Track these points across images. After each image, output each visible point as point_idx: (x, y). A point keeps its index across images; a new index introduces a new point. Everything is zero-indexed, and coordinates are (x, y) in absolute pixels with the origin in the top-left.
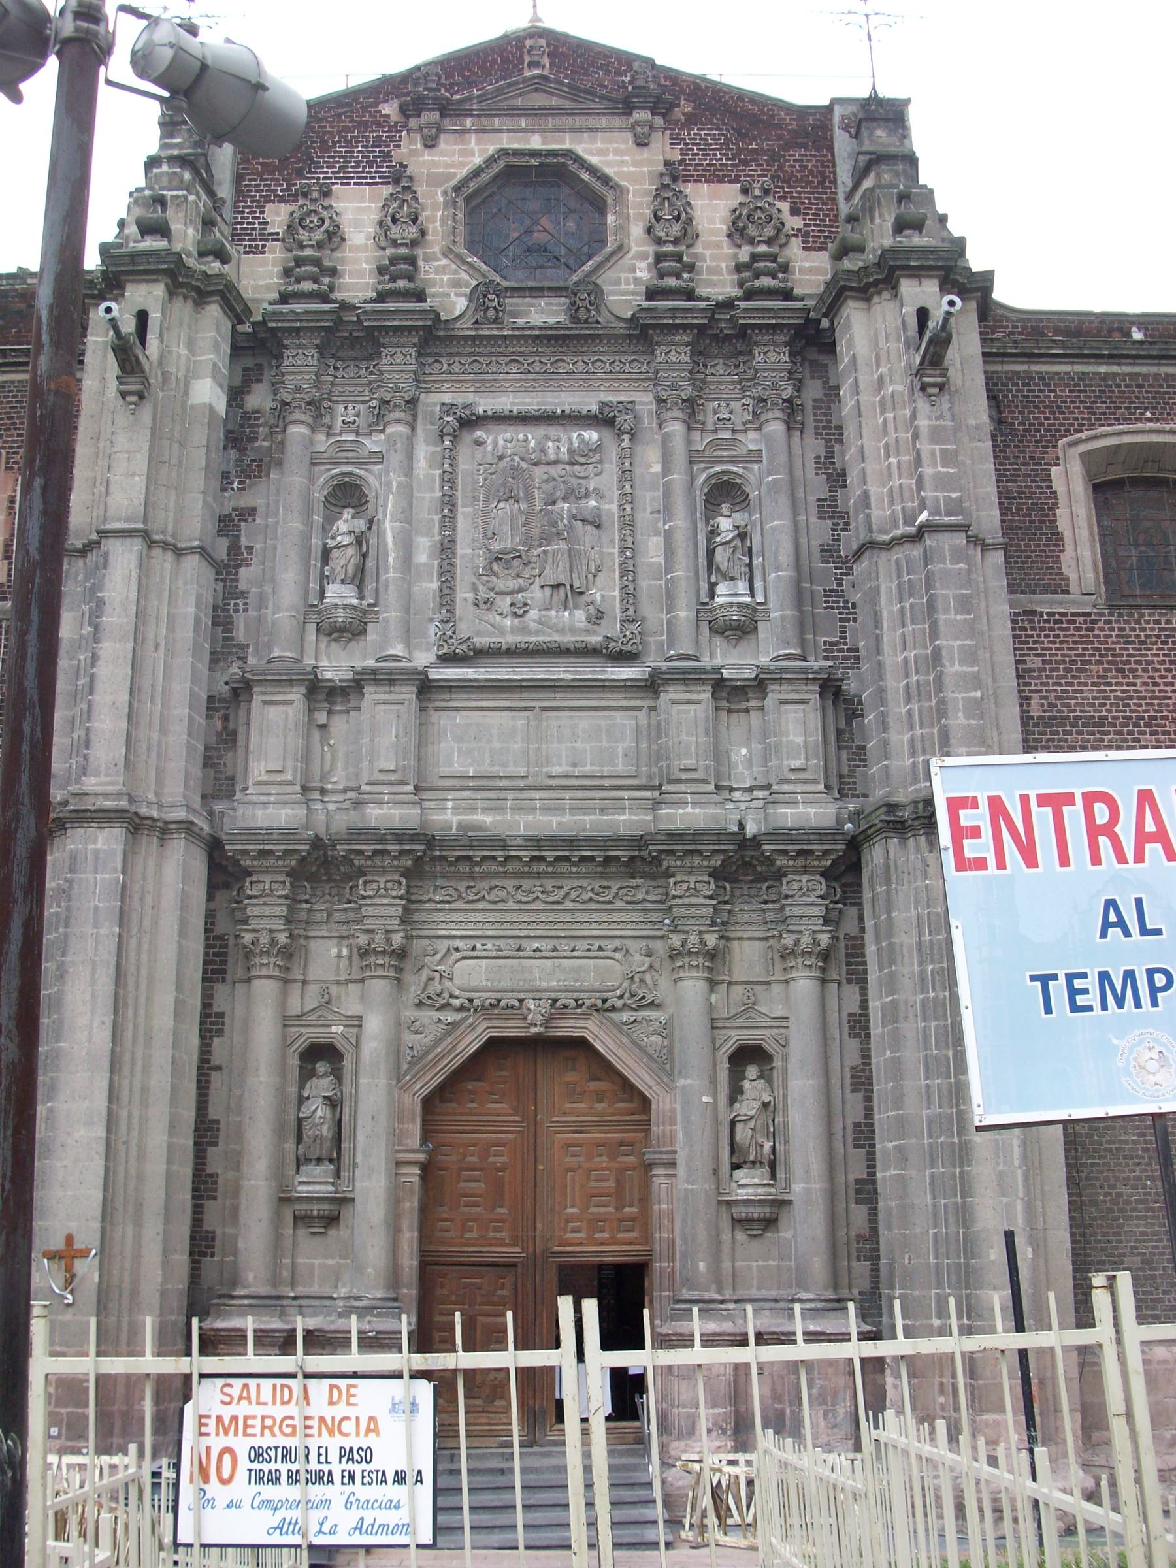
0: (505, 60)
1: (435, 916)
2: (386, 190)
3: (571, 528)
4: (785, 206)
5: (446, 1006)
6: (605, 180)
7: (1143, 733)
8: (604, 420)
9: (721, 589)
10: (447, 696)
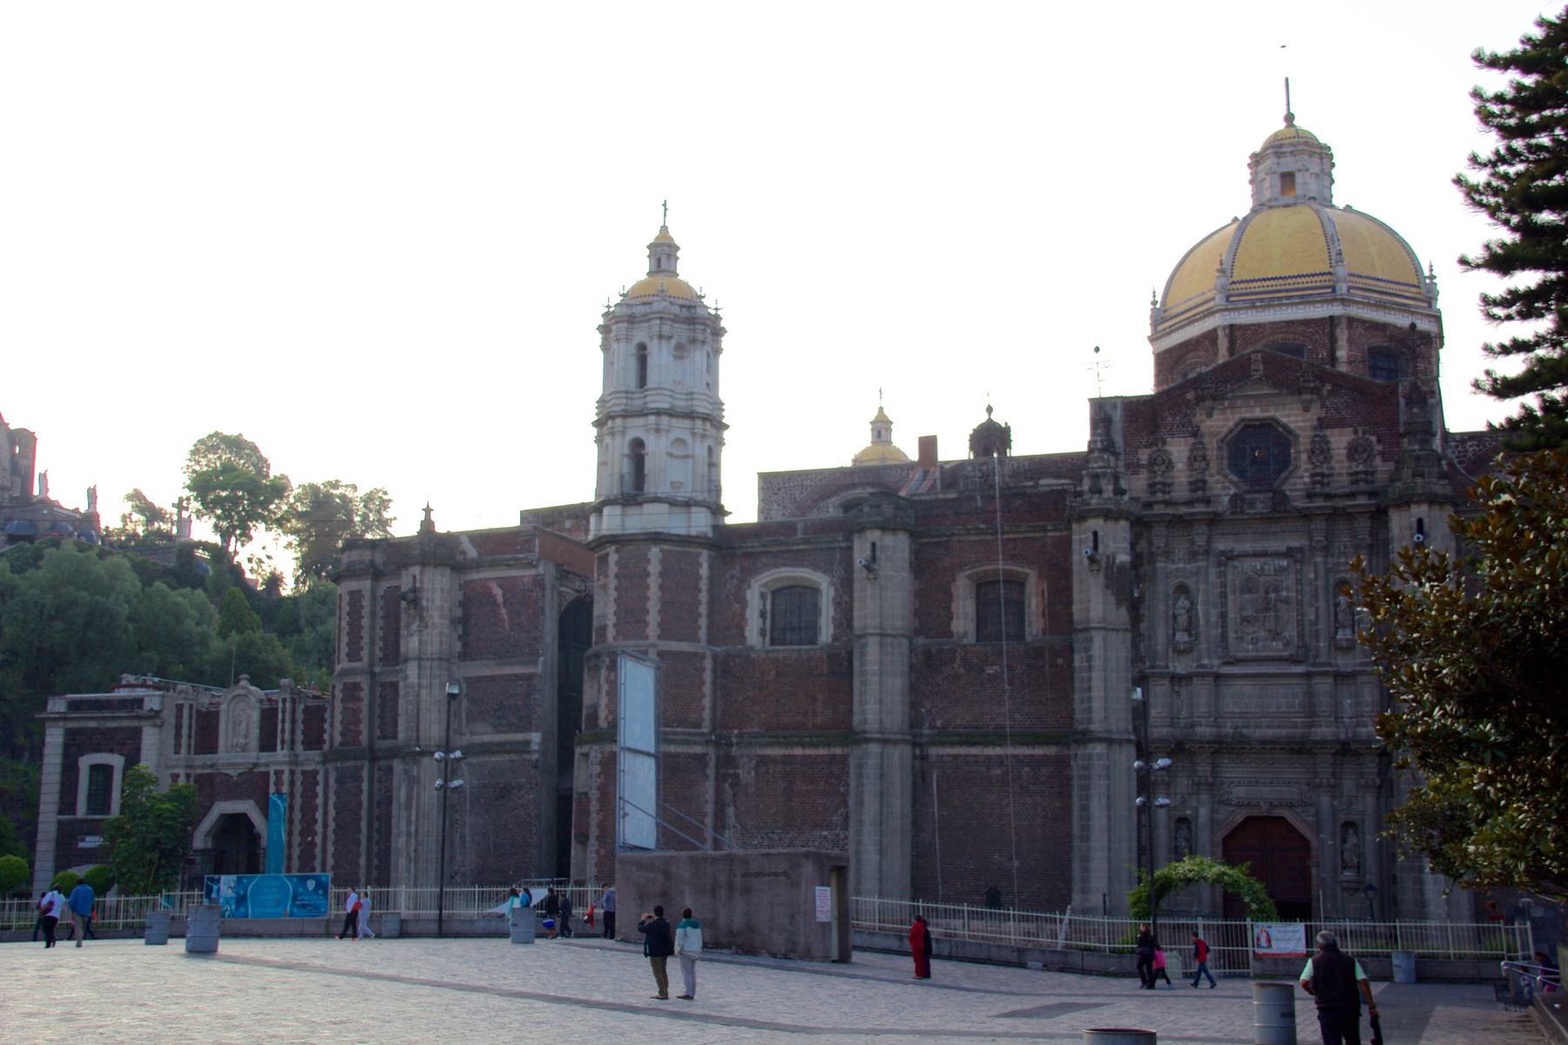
2: (1191, 440)
3: (1275, 606)
4: (1374, 439)
6: (1290, 432)
8: (1289, 553)
9: (1340, 632)
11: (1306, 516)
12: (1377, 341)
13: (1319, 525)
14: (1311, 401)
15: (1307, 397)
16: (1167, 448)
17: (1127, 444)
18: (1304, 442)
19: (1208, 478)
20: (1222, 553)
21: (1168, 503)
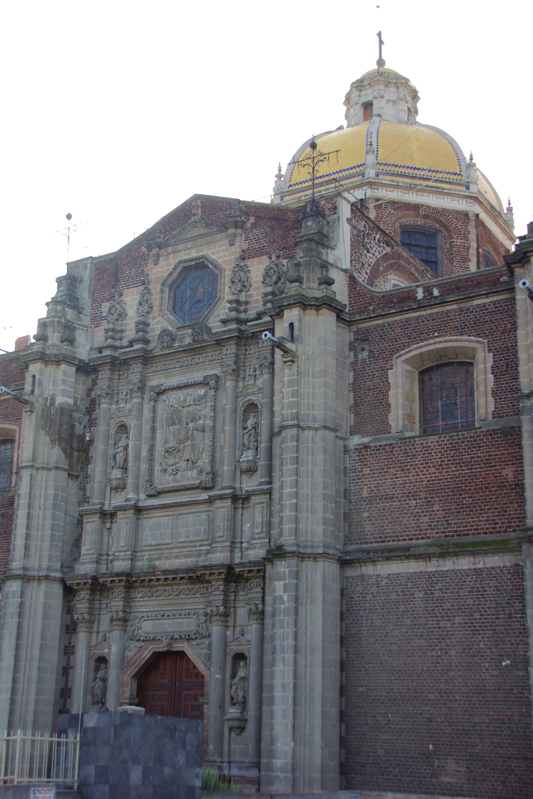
0: (185, 215)
1: (138, 604)
2: (142, 288)
3: (193, 434)
5: (138, 640)
7: (411, 500)
8: (204, 383)
10: (148, 512)
11: (220, 343)
12: (410, 220)
13: (231, 349)
14: (235, 235)
15: (231, 231)
16: (123, 298)
17: (94, 301)
18: (228, 274)
19: (150, 321)
20: (152, 388)
21: (115, 348)
